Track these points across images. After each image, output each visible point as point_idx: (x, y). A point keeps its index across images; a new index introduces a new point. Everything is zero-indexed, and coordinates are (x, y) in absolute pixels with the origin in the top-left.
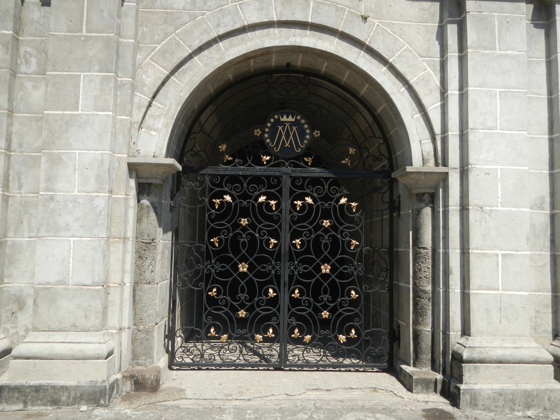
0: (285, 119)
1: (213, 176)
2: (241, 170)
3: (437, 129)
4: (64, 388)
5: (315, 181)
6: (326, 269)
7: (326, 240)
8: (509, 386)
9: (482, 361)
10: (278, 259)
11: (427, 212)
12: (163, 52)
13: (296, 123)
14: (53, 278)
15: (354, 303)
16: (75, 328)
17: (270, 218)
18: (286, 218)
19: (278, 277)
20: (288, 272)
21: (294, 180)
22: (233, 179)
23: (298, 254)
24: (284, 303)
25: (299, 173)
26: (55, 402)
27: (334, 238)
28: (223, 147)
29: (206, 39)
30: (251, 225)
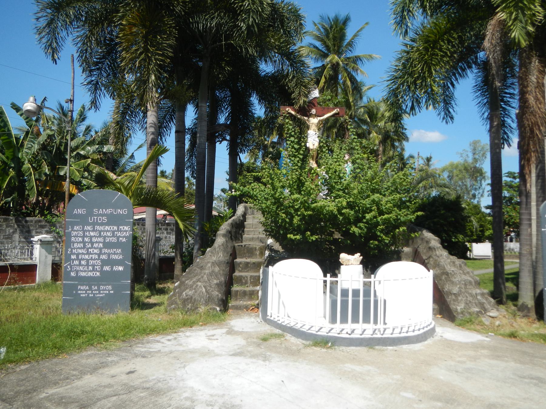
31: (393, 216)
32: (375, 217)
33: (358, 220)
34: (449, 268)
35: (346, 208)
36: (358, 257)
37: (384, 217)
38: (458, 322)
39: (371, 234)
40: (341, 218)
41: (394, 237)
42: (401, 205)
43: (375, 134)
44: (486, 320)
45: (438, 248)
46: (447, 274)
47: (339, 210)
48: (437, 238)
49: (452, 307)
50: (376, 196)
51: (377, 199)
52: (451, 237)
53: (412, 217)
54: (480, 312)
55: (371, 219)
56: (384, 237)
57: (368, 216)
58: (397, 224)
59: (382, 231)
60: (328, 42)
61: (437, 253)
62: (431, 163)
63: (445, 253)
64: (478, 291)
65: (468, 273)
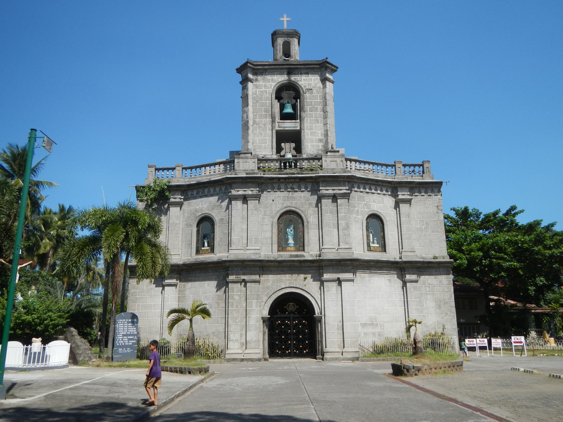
0: (291, 304)
1: (276, 317)
2: (282, 315)
3: (320, 307)
4: (254, 359)
5: (297, 318)
6: (301, 337)
7: (300, 330)
8: (333, 357)
9: (328, 352)
10: (290, 335)
11: (319, 324)
12: (267, 294)
13: (293, 305)
14: (250, 339)
15: (307, 344)
16: (254, 348)
17: (288, 326)
18: (292, 326)
19: (291, 339)
20: (292, 338)
21: (293, 317)
22: (280, 318)
23: (295, 334)
24: (292, 344)
25: (295, 316)
26: (252, 361)
27: (302, 330)
28: (278, 311)
29: (275, 291)
30: (284, 328)
31: (56, 322)
32: (49, 322)
33: (40, 324)
34: (79, 344)
35: (36, 319)
36: (40, 339)
37: (52, 322)
38: (79, 364)
39: (46, 329)
40: (33, 323)
41: (56, 331)
42: (60, 317)
43: (47, 241)
44: (90, 363)
45: (76, 335)
46: (78, 346)
47: (33, 320)
48: (76, 331)
49: (78, 359)
50: (50, 314)
51: (50, 315)
52: (84, 330)
53: (65, 322)
54: (89, 360)
55: (47, 323)
56: (52, 331)
57: (46, 322)
58: (58, 325)
59: (51, 328)
60: (14, 165)
61: (75, 337)
62: (98, 262)
63: (79, 337)
64: (90, 352)
65: (87, 345)
